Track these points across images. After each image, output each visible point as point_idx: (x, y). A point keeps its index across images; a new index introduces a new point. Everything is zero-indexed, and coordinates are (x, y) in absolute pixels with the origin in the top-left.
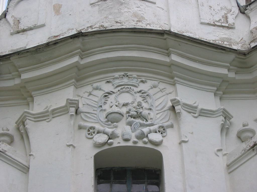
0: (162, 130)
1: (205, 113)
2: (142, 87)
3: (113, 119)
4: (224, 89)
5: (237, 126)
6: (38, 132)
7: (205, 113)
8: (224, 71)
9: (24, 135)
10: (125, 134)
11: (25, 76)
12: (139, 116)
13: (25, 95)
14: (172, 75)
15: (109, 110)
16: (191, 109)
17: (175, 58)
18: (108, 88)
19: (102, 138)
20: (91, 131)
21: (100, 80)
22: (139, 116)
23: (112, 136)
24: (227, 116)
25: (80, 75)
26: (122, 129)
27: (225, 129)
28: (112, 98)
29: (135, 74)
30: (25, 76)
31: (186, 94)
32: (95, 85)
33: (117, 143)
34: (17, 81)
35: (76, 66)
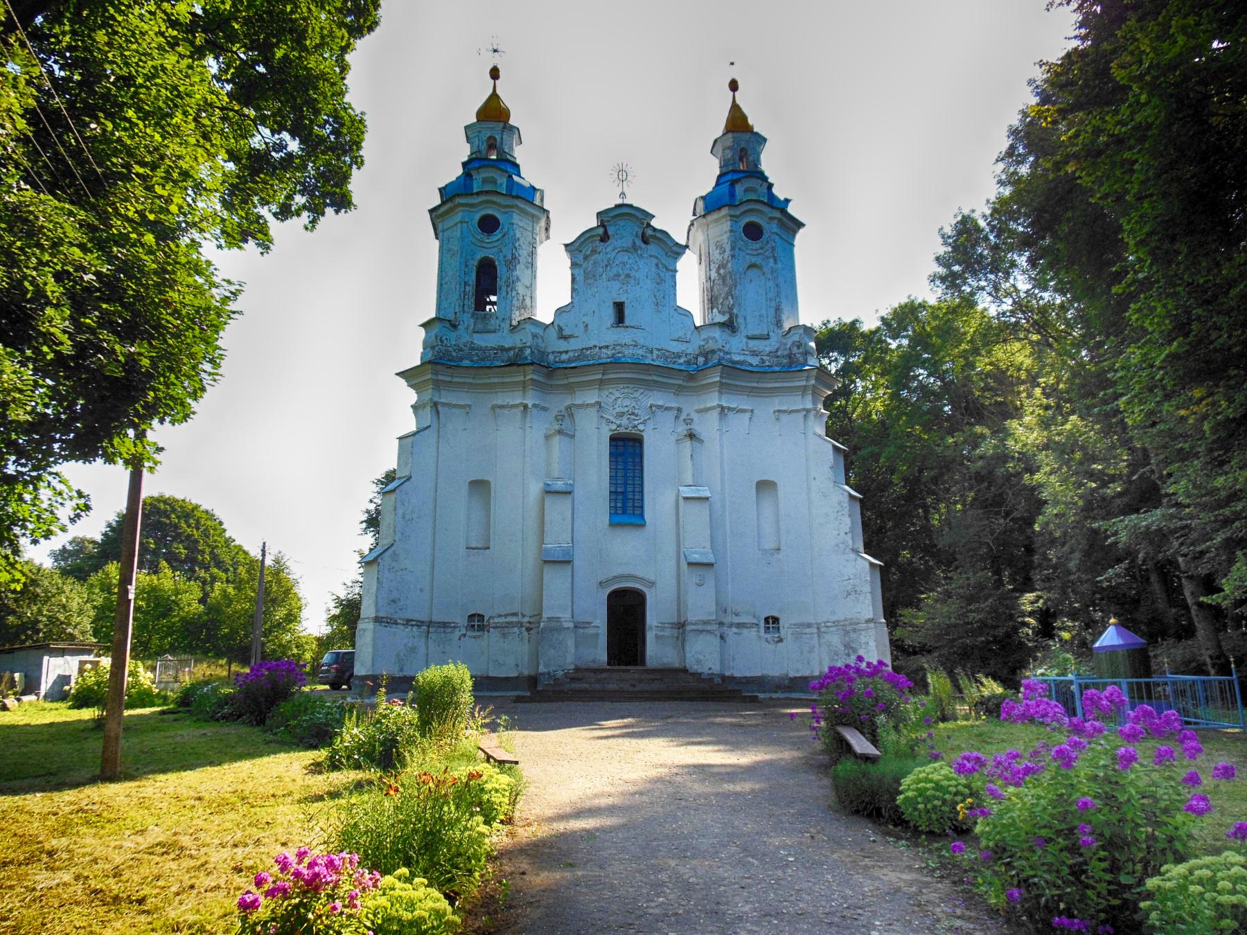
0: (644, 423)
1: (667, 409)
2: (636, 395)
3: (621, 415)
4: (679, 390)
5: (683, 416)
6: (580, 416)
7: (667, 409)
8: (681, 382)
9: (571, 415)
10: (625, 425)
11: (571, 380)
12: (633, 414)
13: (570, 389)
14: (650, 385)
15: (618, 410)
16: (659, 407)
17: (655, 378)
18: (617, 394)
19: (614, 427)
20: (609, 422)
22: (633, 414)
23: (619, 426)
24: (679, 410)
25: (602, 383)
26: (624, 421)
27: (677, 417)
28: (619, 401)
30: (571, 380)
31: (657, 398)
33: (622, 430)
35: (601, 380)
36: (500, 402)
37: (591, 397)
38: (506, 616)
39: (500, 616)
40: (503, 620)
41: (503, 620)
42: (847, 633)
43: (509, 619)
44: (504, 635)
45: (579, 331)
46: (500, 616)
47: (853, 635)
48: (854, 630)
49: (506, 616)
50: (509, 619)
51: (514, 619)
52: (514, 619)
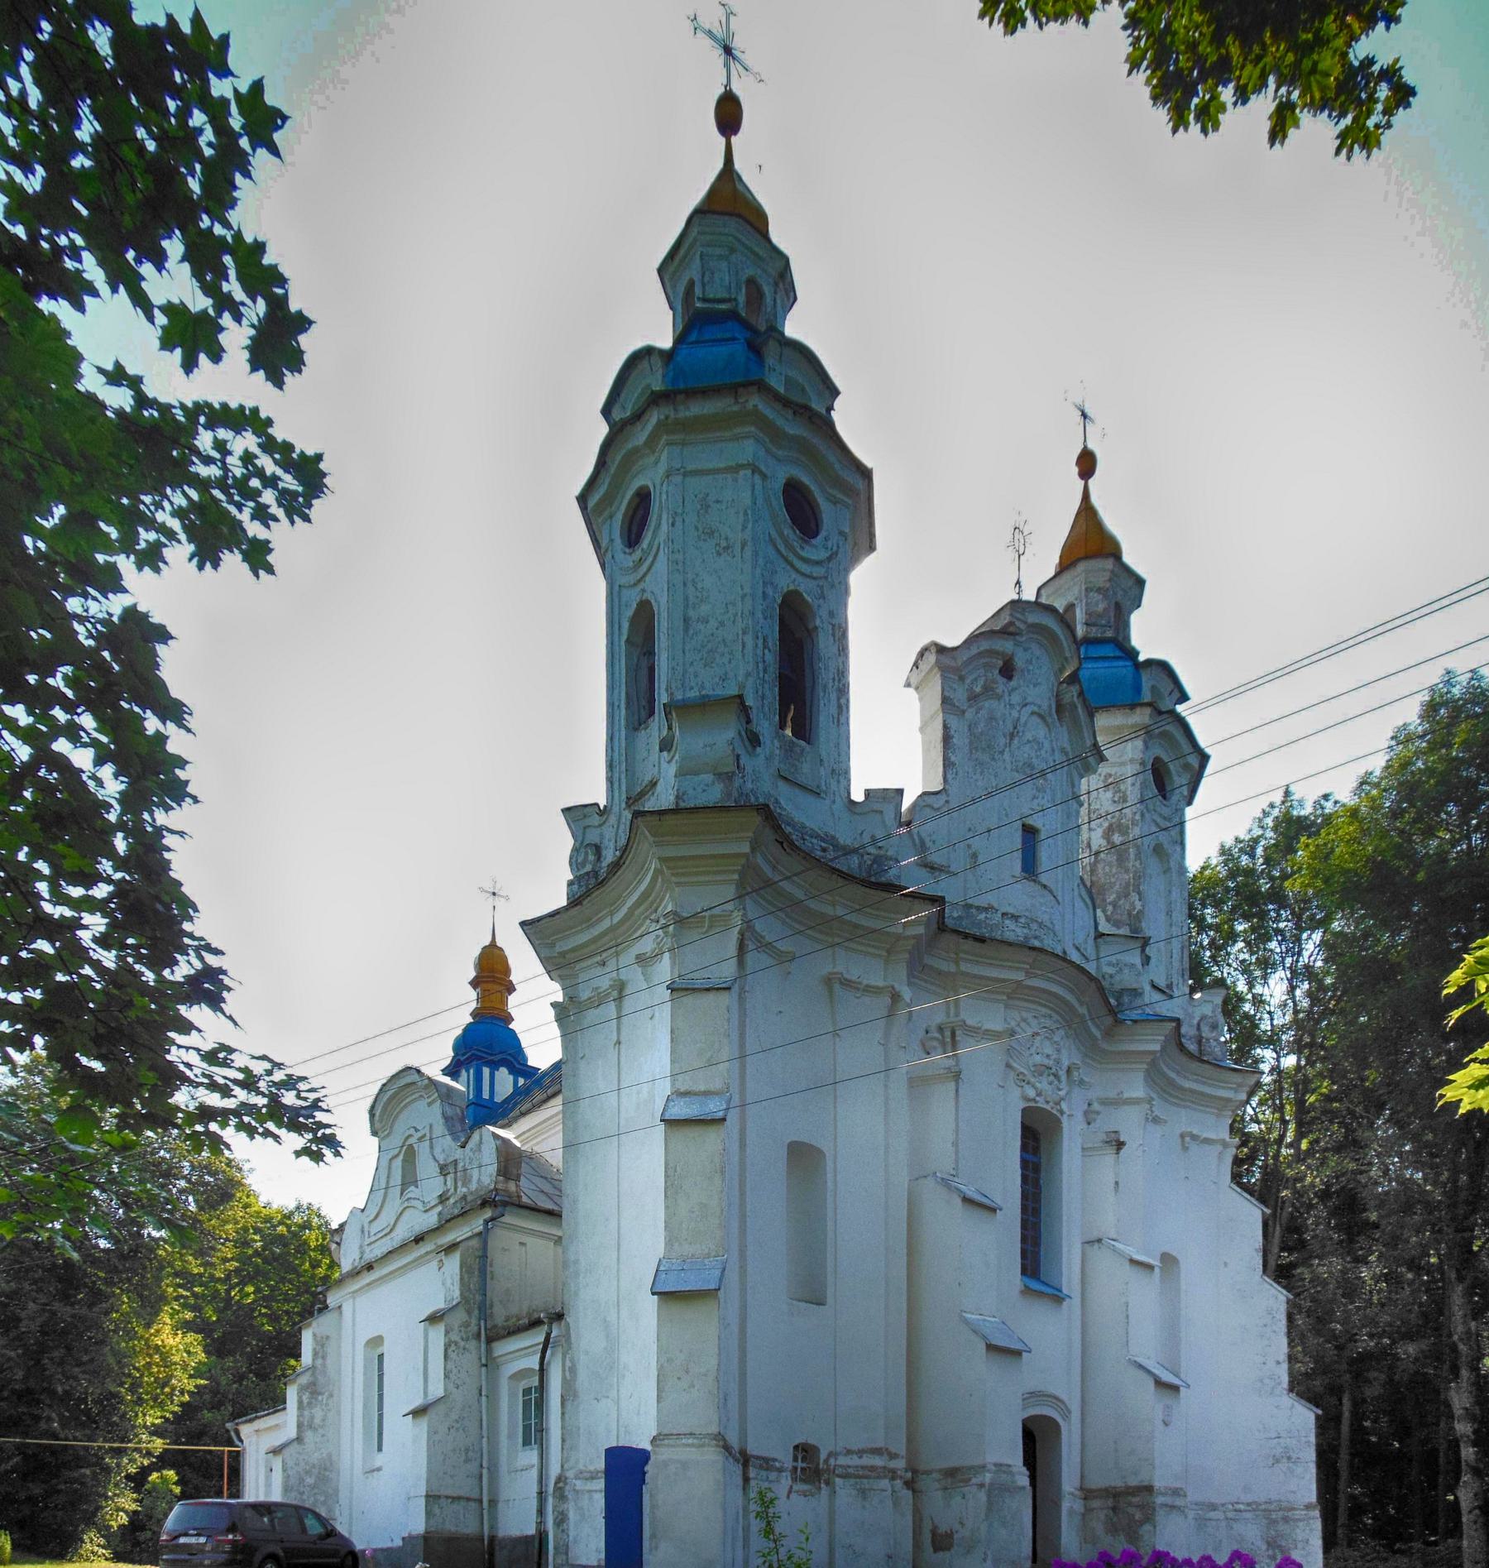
11: (964, 967)
21: (1028, 1010)
29: (1056, 1017)
30: (964, 967)
32: (1024, 1014)
34: (953, 968)
36: (854, 974)
37: (993, 1018)
38: (861, 1453)
39: (849, 1452)
40: (854, 1461)
41: (854, 1461)
42: (1273, 1522)
43: (868, 1460)
44: (863, 1493)
45: (959, 861)
46: (849, 1452)
47: (1281, 1527)
48: (1286, 1520)
49: (861, 1453)
50: (868, 1460)
51: (878, 1461)
52: (878, 1461)
